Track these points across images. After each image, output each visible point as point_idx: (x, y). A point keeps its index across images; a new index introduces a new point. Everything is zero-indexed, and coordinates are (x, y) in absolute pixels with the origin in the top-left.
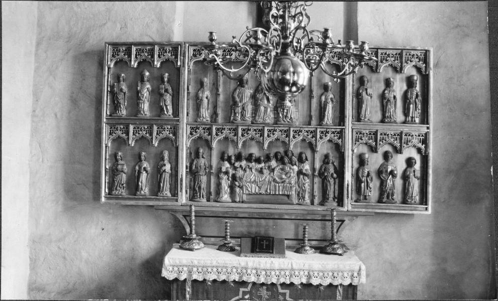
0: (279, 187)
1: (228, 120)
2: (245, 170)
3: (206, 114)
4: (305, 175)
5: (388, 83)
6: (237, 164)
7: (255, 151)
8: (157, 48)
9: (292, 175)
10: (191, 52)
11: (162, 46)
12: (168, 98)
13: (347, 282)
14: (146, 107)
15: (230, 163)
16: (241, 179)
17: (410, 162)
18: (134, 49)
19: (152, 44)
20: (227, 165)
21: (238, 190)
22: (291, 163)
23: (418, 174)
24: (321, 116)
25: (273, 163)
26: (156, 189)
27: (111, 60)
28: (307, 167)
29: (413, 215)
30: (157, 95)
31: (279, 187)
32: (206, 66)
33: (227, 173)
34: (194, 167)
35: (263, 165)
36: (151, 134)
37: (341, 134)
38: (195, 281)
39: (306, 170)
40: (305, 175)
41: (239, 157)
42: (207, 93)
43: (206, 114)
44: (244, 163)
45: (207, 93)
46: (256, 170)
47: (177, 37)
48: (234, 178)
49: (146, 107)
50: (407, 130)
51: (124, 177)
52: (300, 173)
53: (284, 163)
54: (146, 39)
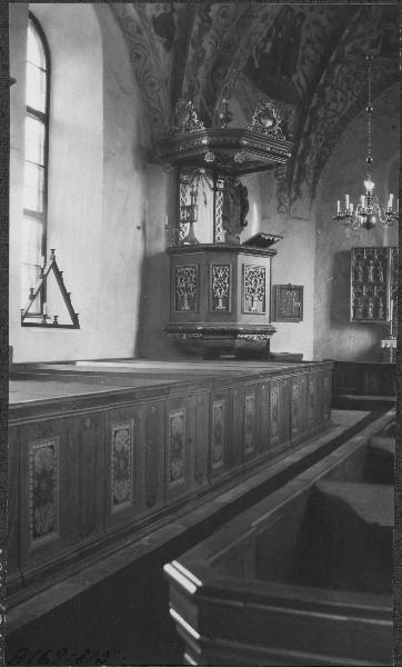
14: (371, 277)
19: (373, 248)
30: (376, 273)
49: (371, 277)
51: (361, 310)
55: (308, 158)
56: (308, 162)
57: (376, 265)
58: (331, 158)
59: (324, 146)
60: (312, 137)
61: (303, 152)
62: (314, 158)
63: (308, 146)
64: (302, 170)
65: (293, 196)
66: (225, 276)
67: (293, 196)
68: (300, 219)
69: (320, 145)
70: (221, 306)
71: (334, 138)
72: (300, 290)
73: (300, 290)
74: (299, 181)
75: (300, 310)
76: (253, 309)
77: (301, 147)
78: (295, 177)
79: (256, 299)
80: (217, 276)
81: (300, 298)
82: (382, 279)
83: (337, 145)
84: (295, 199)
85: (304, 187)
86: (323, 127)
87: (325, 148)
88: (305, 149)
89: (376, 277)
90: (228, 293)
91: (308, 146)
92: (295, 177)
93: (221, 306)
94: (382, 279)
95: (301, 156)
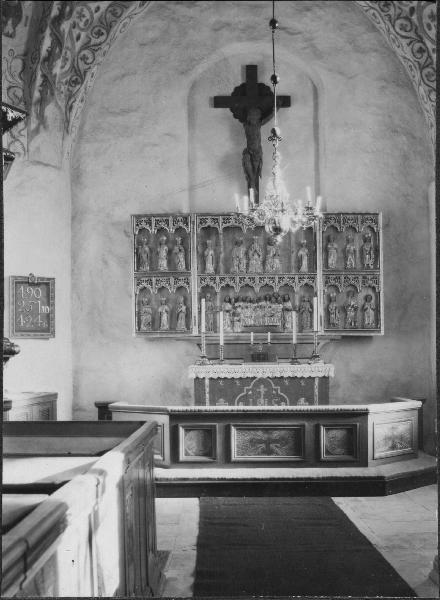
1: (227, 271)
3: (210, 267)
4: (288, 310)
6: (236, 305)
7: (250, 294)
8: (170, 219)
10: (199, 221)
11: (175, 217)
12: (181, 257)
13: (321, 375)
18: (153, 219)
19: (166, 215)
23: (373, 307)
24: (299, 268)
26: (173, 328)
29: (371, 337)
32: (208, 231)
37: (313, 278)
38: (211, 379)
41: (237, 300)
42: (211, 252)
43: (210, 267)
45: (210, 252)
47: (185, 211)
49: (163, 264)
50: (308, 189)
54: (161, 212)
55: (59, 63)
56: (57, 70)
57: (170, 242)
58: (94, 69)
60: (65, 26)
61: (50, 53)
62: (67, 67)
63: (58, 41)
64: (47, 81)
65: (33, 126)
67: (33, 126)
68: (46, 165)
69: (78, 45)
71: (100, 34)
72: (47, 285)
73: (47, 285)
74: (42, 102)
75: (49, 317)
77: (47, 43)
78: (37, 95)
81: (49, 298)
82: (182, 267)
83: (105, 47)
84: (37, 131)
85: (50, 111)
86: (81, 16)
87: (85, 52)
88: (52, 47)
89: (169, 262)
91: (58, 41)
92: (37, 95)
94: (182, 267)
95: (46, 59)
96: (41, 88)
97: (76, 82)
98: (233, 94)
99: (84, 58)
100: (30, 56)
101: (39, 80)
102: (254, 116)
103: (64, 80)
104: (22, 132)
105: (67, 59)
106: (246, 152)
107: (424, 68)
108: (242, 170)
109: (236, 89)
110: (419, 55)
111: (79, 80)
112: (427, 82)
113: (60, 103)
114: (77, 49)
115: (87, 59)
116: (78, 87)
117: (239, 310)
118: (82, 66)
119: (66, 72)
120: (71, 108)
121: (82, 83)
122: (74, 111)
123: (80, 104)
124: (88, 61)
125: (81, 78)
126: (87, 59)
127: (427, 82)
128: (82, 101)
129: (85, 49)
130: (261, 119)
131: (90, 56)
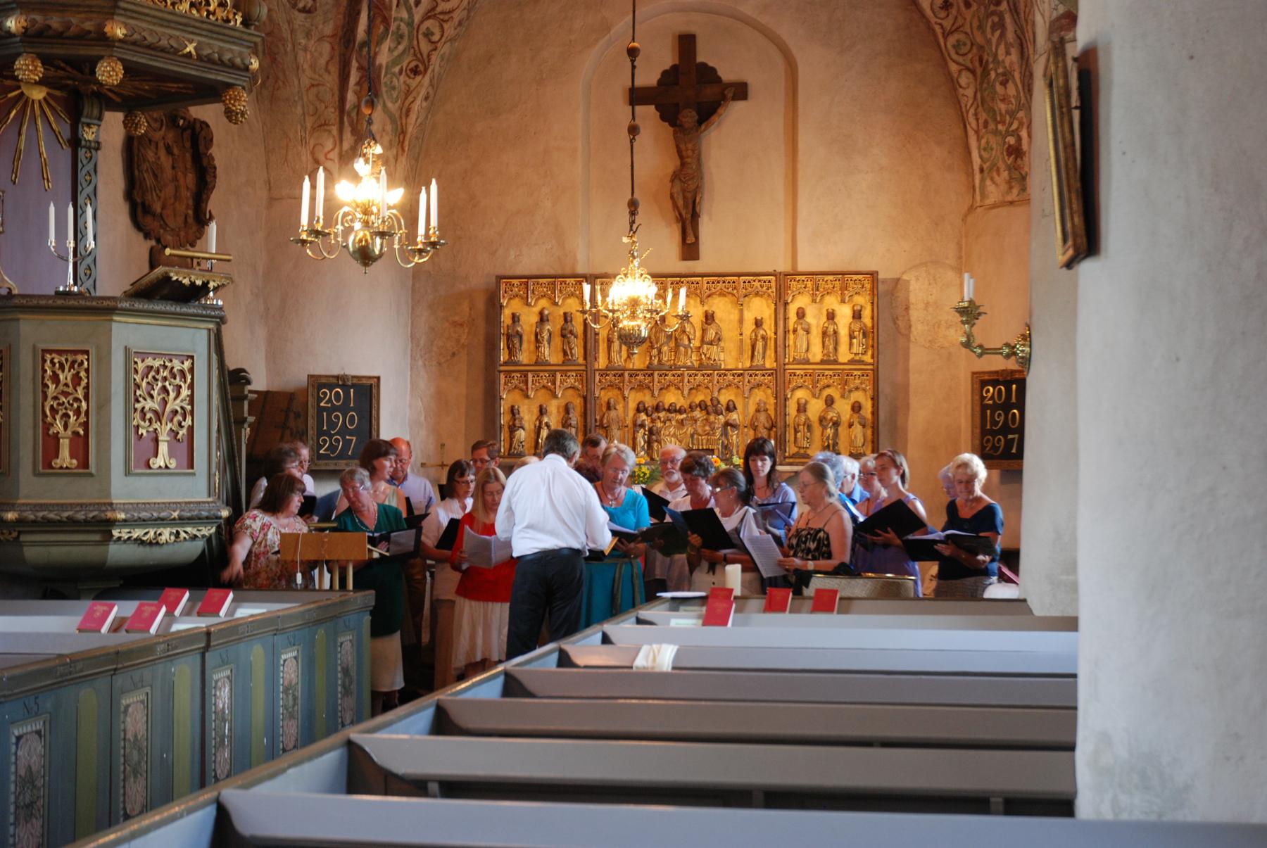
0: (702, 440)
2: (664, 422)
5: (831, 316)
6: (655, 415)
9: (717, 426)
15: (647, 415)
16: (659, 432)
17: (856, 408)
20: (643, 416)
21: (655, 445)
22: (718, 413)
25: (697, 414)
27: (504, 297)
28: (734, 416)
31: (702, 440)
33: (642, 426)
34: (605, 421)
35: (684, 416)
36: (554, 383)
39: (735, 420)
40: (734, 426)
41: (657, 408)
44: (662, 414)
46: (677, 421)
48: (651, 432)
52: (727, 424)
53: (708, 413)
59: (427, 17)
66: (77, 379)
70: (65, 458)
76: (159, 461)
79: (164, 437)
80: (55, 379)
87: (429, 23)
90: (86, 425)
93: (65, 458)
96: (358, 88)
97: (415, 71)
98: (660, 82)
99: (428, 34)
100: (346, 36)
101: (354, 77)
102: (689, 117)
103: (397, 69)
104: (331, 155)
105: (401, 37)
106: (675, 177)
107: (951, 33)
108: (669, 205)
109: (665, 74)
110: (943, 14)
111: (421, 68)
112: (960, 59)
113: (390, 105)
114: (417, 18)
115: (433, 34)
116: (419, 78)
117: (659, 425)
118: (425, 47)
119: (167, 265)
120: (408, 111)
121: (426, 70)
122: (413, 116)
123: (424, 104)
124: (436, 38)
125: (423, 63)
126: (433, 34)
127: (960, 59)
128: (426, 99)
129: (429, 18)
130: (700, 122)
131: (437, 31)
